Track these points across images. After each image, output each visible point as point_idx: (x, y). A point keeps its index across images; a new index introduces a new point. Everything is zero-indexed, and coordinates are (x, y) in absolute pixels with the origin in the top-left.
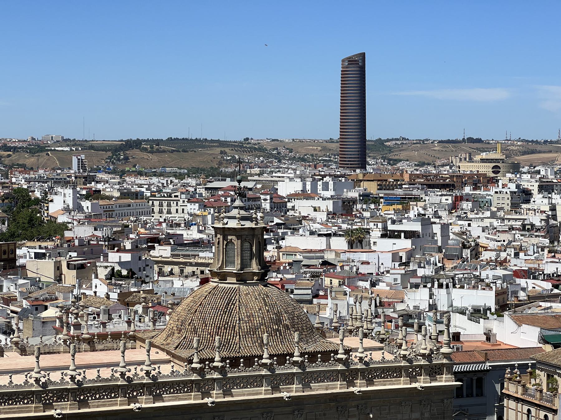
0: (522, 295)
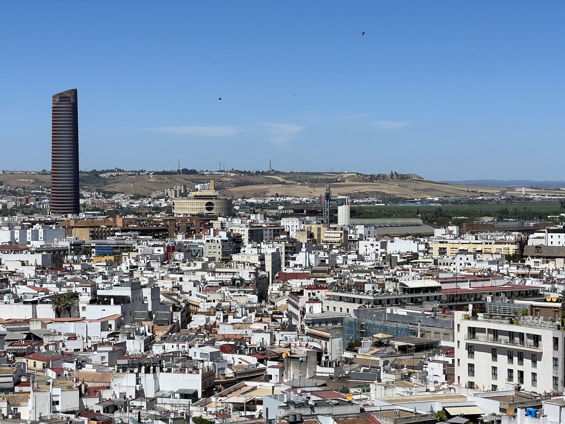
0: (229, 373)
